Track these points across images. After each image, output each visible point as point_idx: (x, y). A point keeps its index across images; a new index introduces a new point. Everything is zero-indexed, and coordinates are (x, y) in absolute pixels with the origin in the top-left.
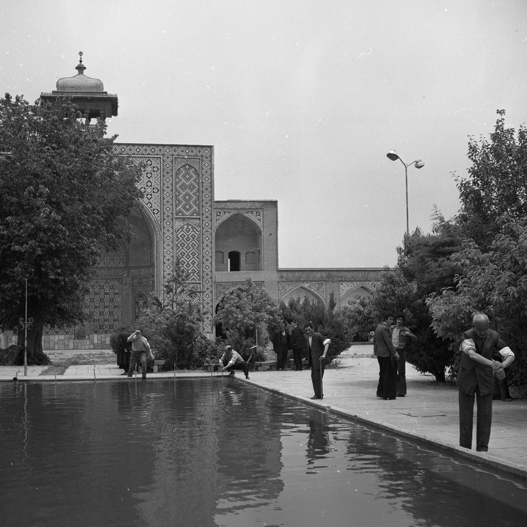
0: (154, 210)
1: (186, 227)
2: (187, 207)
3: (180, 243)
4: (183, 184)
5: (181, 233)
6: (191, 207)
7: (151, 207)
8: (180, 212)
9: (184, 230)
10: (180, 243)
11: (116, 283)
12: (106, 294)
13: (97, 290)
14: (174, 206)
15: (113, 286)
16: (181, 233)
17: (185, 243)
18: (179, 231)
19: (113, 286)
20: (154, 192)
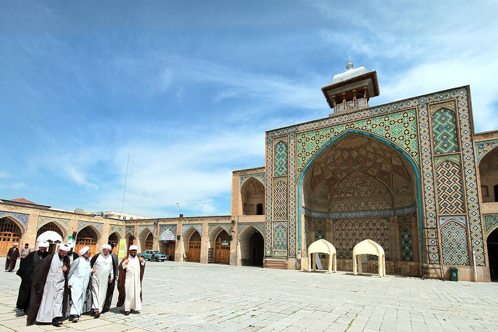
0: (412, 153)
1: (445, 164)
2: (445, 145)
3: (441, 179)
4: (440, 126)
5: (441, 170)
6: (449, 145)
7: (410, 151)
8: (438, 151)
9: (443, 166)
10: (441, 179)
12: (378, 229)
13: (371, 227)
14: (432, 147)
16: (441, 170)
17: (446, 178)
18: (439, 168)
19: (383, 224)
20: (411, 138)
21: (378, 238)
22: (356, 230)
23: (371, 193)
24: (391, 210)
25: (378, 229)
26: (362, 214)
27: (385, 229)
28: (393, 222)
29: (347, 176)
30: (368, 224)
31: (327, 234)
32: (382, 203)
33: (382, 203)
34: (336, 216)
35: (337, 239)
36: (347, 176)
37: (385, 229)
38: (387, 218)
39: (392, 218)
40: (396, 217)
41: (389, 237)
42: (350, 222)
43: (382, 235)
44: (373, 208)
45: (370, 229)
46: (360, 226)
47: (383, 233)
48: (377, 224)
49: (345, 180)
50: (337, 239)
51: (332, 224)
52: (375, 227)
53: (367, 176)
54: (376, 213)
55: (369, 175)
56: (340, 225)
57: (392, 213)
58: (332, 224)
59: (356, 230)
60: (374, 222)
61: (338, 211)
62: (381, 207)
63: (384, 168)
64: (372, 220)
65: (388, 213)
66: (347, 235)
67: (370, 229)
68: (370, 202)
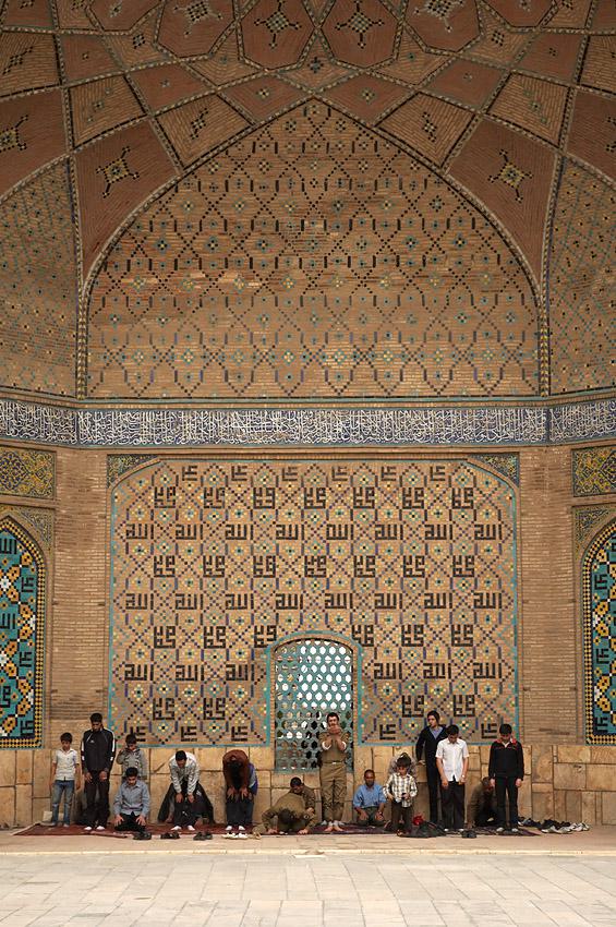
11: (484, 480)
12: (433, 533)
15: (469, 493)
19: (469, 493)
21: (435, 589)
22: (284, 534)
23: (397, 276)
24: (524, 402)
25: (433, 533)
26: (330, 426)
27: (481, 533)
28: (538, 483)
29: (243, 134)
30: (370, 492)
31: (61, 560)
32: (468, 357)
33: (468, 357)
34: (144, 427)
35: (135, 602)
36: (243, 134)
37: (481, 533)
38: (499, 458)
39: (529, 460)
40: (560, 454)
41: (509, 587)
42: (237, 474)
43: (463, 568)
44: (413, 383)
45: (384, 533)
46: (309, 505)
47: (470, 560)
48: (427, 498)
49: (223, 166)
50: (135, 602)
51: (98, 488)
52: (414, 518)
53: (387, 152)
54: (425, 424)
55: (402, 148)
56: (166, 497)
57: (534, 422)
58: (98, 488)
59: (284, 534)
60: (413, 480)
61: (154, 391)
62: (463, 383)
63: (514, 110)
64: (400, 467)
65: (506, 425)
66: (214, 567)
67: (384, 533)
68: (393, 344)
